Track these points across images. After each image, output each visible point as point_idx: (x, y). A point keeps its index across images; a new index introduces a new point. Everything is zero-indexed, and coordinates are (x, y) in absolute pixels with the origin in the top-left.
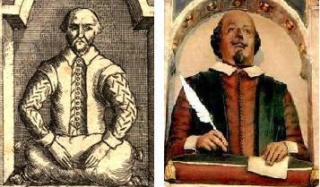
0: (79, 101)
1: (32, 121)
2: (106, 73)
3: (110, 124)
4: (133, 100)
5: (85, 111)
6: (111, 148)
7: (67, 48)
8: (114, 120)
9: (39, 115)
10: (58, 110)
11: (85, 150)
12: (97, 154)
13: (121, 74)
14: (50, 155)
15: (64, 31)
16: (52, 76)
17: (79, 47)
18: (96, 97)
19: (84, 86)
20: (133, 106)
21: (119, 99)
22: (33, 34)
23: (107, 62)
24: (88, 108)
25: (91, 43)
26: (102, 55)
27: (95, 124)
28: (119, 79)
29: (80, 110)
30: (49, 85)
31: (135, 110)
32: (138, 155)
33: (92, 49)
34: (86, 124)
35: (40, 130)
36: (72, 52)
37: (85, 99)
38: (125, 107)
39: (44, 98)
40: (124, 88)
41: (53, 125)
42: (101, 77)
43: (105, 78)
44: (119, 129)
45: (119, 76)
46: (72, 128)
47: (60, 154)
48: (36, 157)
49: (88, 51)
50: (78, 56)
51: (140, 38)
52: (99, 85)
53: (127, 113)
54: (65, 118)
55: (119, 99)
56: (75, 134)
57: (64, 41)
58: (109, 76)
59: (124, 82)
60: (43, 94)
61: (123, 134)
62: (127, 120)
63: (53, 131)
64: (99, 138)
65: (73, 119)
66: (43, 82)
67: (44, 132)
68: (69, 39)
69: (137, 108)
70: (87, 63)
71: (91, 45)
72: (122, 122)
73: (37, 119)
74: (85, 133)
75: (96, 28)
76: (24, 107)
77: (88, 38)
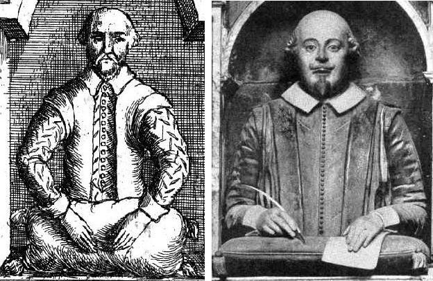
0: (106, 148)
1: (37, 178)
2: (145, 107)
3: (150, 182)
4: (184, 146)
5: (113, 163)
6: (152, 220)
7: (88, 69)
10: (74, 163)
11: (114, 222)
12: (131, 229)
14: (61, 229)
15: (82, 43)
17: (106, 67)
19: (113, 126)
20: (185, 157)
21: (164, 146)
22: (37, 47)
23: (145, 90)
26: (140, 80)
27: (128, 183)
28: (164, 115)
30: (61, 124)
31: (187, 162)
32: (192, 231)
33: (124, 69)
34: (116, 183)
37: (115, 144)
38: (172, 157)
41: (67, 185)
42: (137, 112)
43: (143, 114)
44: (163, 190)
45: (164, 110)
47: (78, 229)
48: (42, 232)
49: (117, 74)
50: (103, 81)
53: (175, 167)
54: (84, 175)
55: (164, 146)
56: (98, 199)
57: (81, 59)
60: (52, 139)
61: (169, 200)
62: (175, 177)
63: (68, 194)
64: (134, 204)
66: (52, 120)
67: (53, 196)
68: (91, 55)
70: (117, 91)
71: (122, 64)
72: (167, 180)
73: (44, 178)
74: (114, 196)
75: (130, 39)
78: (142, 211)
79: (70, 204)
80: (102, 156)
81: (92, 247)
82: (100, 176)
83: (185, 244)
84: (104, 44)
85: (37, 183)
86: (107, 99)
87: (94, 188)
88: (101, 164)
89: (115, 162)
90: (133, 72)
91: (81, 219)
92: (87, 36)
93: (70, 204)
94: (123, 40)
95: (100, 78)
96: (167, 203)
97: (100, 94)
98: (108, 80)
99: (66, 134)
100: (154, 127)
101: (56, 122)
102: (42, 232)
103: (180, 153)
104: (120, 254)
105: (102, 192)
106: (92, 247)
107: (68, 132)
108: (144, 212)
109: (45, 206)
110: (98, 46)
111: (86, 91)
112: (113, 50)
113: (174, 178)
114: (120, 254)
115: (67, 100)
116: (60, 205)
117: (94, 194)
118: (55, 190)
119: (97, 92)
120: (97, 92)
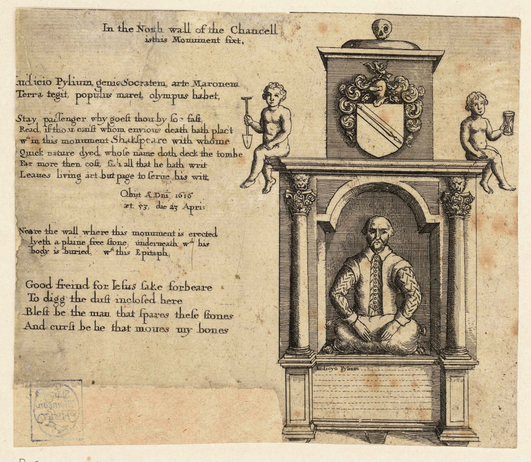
0: (377, 288)
1: (340, 304)
2: (397, 267)
3: (400, 307)
4: (418, 288)
5: (381, 296)
6: (401, 325)
7: (367, 247)
8: (404, 303)
9: (345, 300)
10: (360, 296)
11: (381, 326)
12: (390, 330)
13: (409, 268)
14: (353, 331)
15: (364, 234)
16: (356, 269)
17: (377, 246)
18: (390, 286)
19: (381, 277)
20: (418, 293)
21: (408, 287)
22: (340, 237)
23: (398, 258)
24: (384, 294)
25: (385, 244)
26: (395, 253)
27: (389, 307)
28: (408, 272)
29: (377, 296)
30: (353, 276)
31: (420, 296)
32: (423, 331)
33: (387, 248)
34: (382, 306)
35: (346, 311)
36: (370, 250)
37: (381, 287)
38: (412, 293)
39: (349, 287)
40: (411, 278)
41: (356, 307)
42: (393, 270)
43: (397, 271)
44: (407, 310)
45: (408, 269)
46: (371, 310)
47: (362, 330)
48: (343, 332)
49: (383, 250)
50: (375, 254)
51: (424, 240)
52: (392, 277)
53: (414, 298)
54: (365, 302)
55: (408, 287)
56: (373, 314)
57: (365, 242)
58: (400, 269)
59: (412, 274)
60: (348, 283)
61: (411, 314)
62: (414, 303)
63: (356, 312)
64: (391, 318)
65: (372, 302)
66: (348, 274)
67: (349, 313)
68: (369, 240)
69: (422, 294)
70: (383, 259)
71: (386, 245)
72: (410, 305)
73: (344, 303)
74: (381, 313)
75: (390, 232)
76: (333, 294)
77: (384, 240)
78: (396, 321)
79: (358, 317)
80: (375, 292)
81: (370, 339)
82: (374, 303)
83: (419, 338)
84: (376, 235)
85: (340, 306)
86: (378, 263)
87: (371, 309)
88: (374, 297)
89: (382, 296)
90: (391, 249)
91: (364, 324)
92: (367, 231)
93: (358, 317)
94: (386, 232)
95: (374, 252)
96: (409, 316)
97: (374, 260)
98: (378, 253)
99: (356, 281)
100: (403, 278)
101: (350, 275)
102: (343, 332)
103: (417, 291)
104: (384, 343)
105: (375, 311)
106: (370, 339)
107: (357, 280)
108: (397, 321)
109: (345, 318)
110: (373, 236)
111: (366, 259)
112: (380, 238)
113: (413, 304)
114: (384, 343)
115: (356, 264)
116: (353, 318)
117: (371, 312)
118: (349, 310)
119: (372, 259)
120: (372, 259)
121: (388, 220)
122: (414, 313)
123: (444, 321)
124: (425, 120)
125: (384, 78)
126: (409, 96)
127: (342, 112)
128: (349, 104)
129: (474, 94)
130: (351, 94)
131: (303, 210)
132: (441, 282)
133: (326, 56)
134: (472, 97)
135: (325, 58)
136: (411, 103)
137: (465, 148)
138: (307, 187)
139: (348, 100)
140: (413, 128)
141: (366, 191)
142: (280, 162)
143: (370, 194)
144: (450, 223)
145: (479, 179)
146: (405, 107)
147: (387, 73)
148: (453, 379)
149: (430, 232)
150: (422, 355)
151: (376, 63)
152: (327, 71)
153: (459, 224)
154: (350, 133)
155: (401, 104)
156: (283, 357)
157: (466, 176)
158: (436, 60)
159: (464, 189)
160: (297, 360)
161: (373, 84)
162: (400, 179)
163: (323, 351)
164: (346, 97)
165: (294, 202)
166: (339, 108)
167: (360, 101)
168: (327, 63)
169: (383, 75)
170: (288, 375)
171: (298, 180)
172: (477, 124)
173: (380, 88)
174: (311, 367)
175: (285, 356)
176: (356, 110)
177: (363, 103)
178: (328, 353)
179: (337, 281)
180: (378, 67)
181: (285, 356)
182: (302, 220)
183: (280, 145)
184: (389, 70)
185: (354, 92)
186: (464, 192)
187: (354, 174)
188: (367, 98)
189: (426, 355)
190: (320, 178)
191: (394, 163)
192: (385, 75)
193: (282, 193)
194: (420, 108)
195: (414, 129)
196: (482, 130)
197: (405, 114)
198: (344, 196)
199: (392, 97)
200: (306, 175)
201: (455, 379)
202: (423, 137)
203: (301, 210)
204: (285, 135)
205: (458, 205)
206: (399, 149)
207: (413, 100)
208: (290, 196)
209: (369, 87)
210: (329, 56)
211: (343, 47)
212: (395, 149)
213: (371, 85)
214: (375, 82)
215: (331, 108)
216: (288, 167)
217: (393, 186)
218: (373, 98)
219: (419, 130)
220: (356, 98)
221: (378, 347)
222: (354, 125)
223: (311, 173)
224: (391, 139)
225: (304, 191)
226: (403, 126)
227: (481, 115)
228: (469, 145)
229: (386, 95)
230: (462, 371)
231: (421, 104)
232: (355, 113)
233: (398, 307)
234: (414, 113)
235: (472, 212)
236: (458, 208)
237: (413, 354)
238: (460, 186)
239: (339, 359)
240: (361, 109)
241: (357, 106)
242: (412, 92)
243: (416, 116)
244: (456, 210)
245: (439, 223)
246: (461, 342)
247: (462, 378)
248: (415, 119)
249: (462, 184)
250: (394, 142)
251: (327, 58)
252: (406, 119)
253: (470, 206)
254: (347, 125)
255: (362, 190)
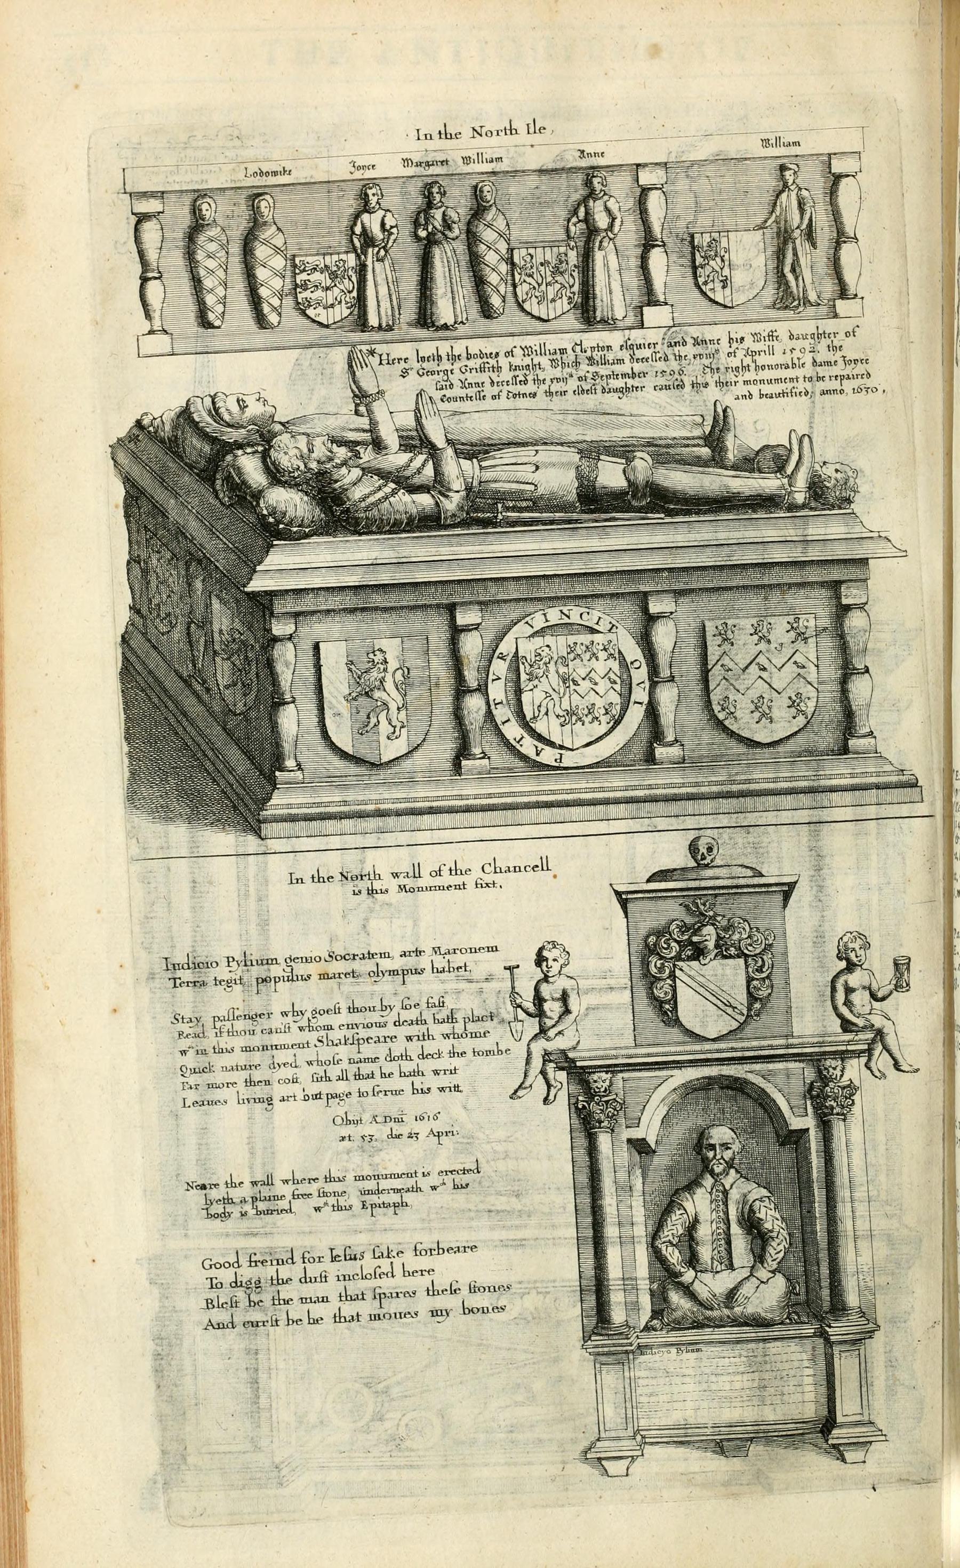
1: (669, 1258)
2: (751, 1198)
3: (760, 1258)
4: (784, 1226)
5: (729, 1243)
6: (762, 1282)
11: (732, 1286)
12: (747, 1289)
17: (717, 1170)
19: (727, 1213)
20: (785, 1233)
21: (768, 1226)
25: (730, 1165)
29: (723, 1242)
33: (732, 1171)
35: (679, 1267)
38: (775, 1234)
40: (772, 1212)
41: (692, 1260)
42: (745, 1203)
44: (769, 1260)
45: (767, 1200)
46: (716, 1263)
48: (675, 1297)
49: (727, 1174)
50: (716, 1181)
52: (742, 1212)
54: (705, 1253)
55: (768, 1226)
56: (719, 1269)
60: (679, 1227)
63: (694, 1268)
66: (678, 1212)
67: (683, 1270)
68: (705, 1162)
69: (789, 1234)
70: (727, 1187)
72: (772, 1252)
73: (674, 1256)
74: (731, 1267)
75: (736, 1147)
76: (658, 1243)
77: (727, 1159)
102: (675, 1297)
104: (738, 1310)
109: (677, 1277)
110: (711, 1154)
111: (703, 1190)
114: (738, 1310)
115: (688, 1196)
121: (733, 1130)
122: (779, 1263)
123: (825, 1271)
124: (778, 980)
125: (713, 921)
126: (751, 945)
127: (654, 977)
128: (663, 964)
129: (849, 935)
130: (665, 949)
131: (605, 1124)
132: (817, 1215)
133: (624, 897)
134: (845, 939)
135: (623, 900)
136: (755, 955)
137: (840, 1016)
138: (608, 1091)
139: (661, 958)
140: (761, 993)
141: (695, 1090)
142: (567, 1057)
143: (701, 1094)
144: (825, 1126)
145: (863, 1060)
146: (746, 962)
147: (716, 915)
148: (843, 1354)
149: (796, 1143)
150: (797, 1323)
151: (698, 901)
152: (626, 917)
153: (838, 1128)
154: (667, 1006)
155: (739, 957)
156: (590, 1339)
157: (843, 1056)
158: (787, 891)
159: (842, 1076)
160: (610, 1342)
161: (697, 932)
162: (747, 1067)
163: (647, 1328)
164: (658, 954)
165: (590, 1114)
166: (648, 970)
167: (678, 957)
168: (626, 908)
169: (711, 918)
170: (598, 1366)
171: (595, 1082)
172: (854, 979)
173: (708, 938)
174: (633, 1352)
175: (593, 1338)
176: (674, 971)
177: (683, 960)
178: (655, 1330)
179: (662, 1226)
180: (702, 907)
181: (593, 1338)
182: (604, 1141)
183: (565, 1032)
184: (719, 909)
185: (669, 945)
186: (843, 1080)
187: (678, 1065)
188: (689, 953)
189: (802, 1323)
190: (626, 1075)
191: (734, 1045)
192: (713, 917)
193: (573, 1101)
194: (768, 962)
195: (763, 993)
196: (864, 988)
197: (747, 972)
198: (663, 1100)
199: (727, 949)
200: (607, 1072)
201: (848, 1354)
202: (777, 1003)
203: (603, 1125)
204: (571, 1017)
205: (835, 1100)
206: (742, 1024)
207: (758, 951)
208: (584, 1106)
209: (690, 937)
210: (630, 896)
211: (648, 881)
212: (735, 1025)
213: (694, 934)
214: (699, 929)
215: (637, 972)
216: (578, 1064)
217: (737, 1079)
218: (698, 953)
219: (770, 994)
220: (673, 954)
221: (728, 1317)
222: (673, 995)
223: (612, 1069)
224: (730, 1010)
225: (604, 1096)
226: (745, 991)
227: (861, 966)
228: (844, 1011)
229: (717, 946)
230: (856, 1342)
231: (770, 956)
232: (673, 976)
233: (754, 1256)
234: (760, 970)
235: (856, 1109)
236: (835, 1105)
237: (782, 1323)
238: (835, 1072)
239: (674, 1337)
240: (681, 970)
241: (675, 965)
242: (755, 939)
243: (764, 975)
244: (832, 1108)
245: (808, 1130)
246: (852, 1299)
247: (857, 1352)
248: (763, 979)
249: (839, 1068)
250: (733, 1014)
251: (627, 899)
252: (749, 980)
253: (853, 1100)
254: (662, 995)
255: (690, 1089)
